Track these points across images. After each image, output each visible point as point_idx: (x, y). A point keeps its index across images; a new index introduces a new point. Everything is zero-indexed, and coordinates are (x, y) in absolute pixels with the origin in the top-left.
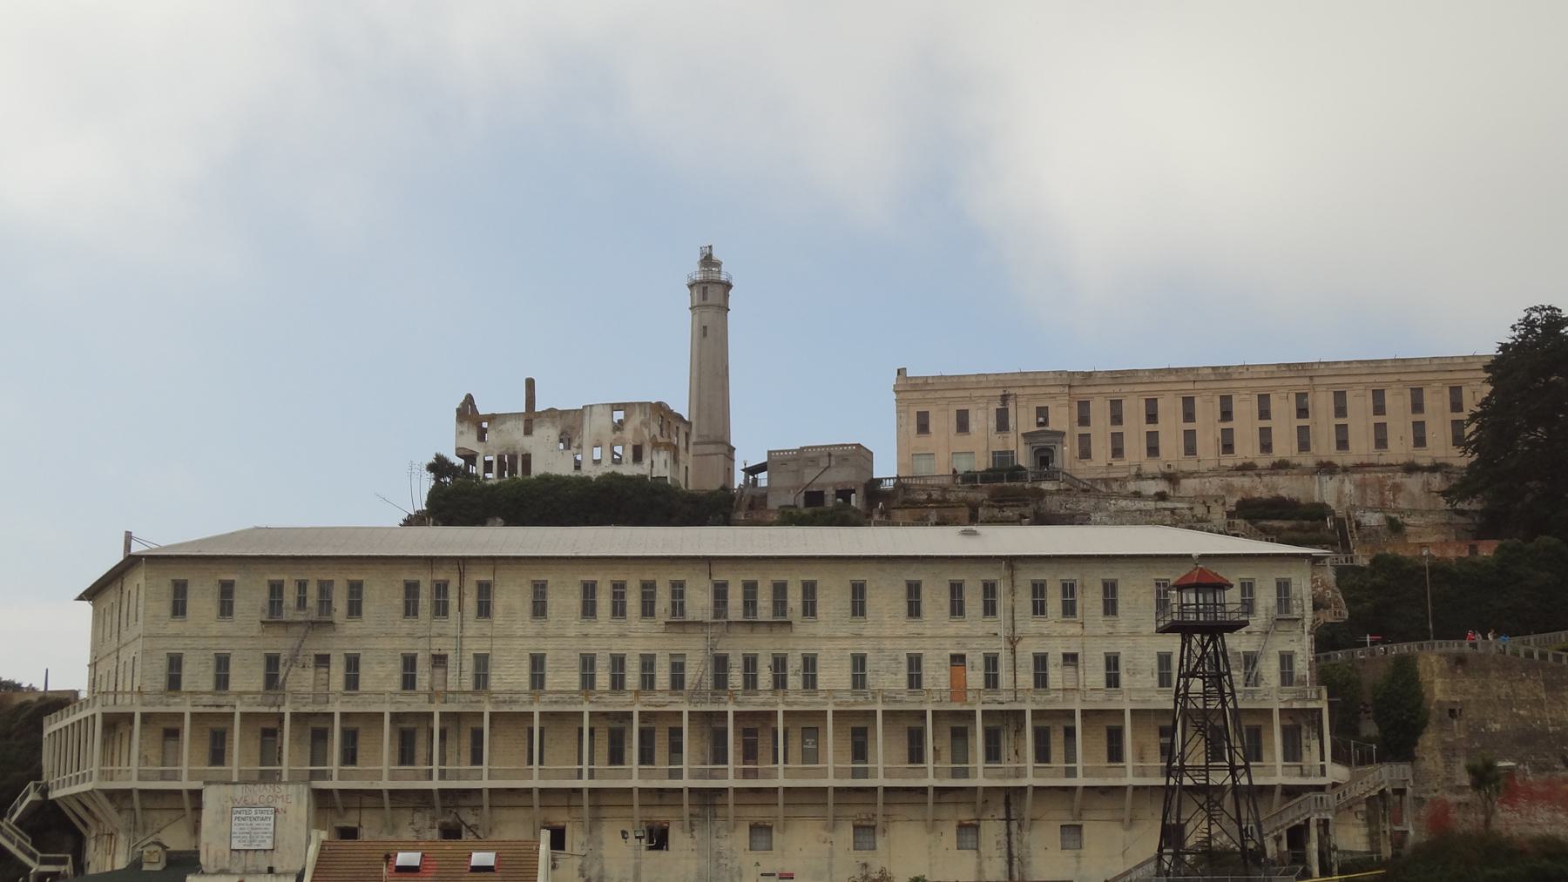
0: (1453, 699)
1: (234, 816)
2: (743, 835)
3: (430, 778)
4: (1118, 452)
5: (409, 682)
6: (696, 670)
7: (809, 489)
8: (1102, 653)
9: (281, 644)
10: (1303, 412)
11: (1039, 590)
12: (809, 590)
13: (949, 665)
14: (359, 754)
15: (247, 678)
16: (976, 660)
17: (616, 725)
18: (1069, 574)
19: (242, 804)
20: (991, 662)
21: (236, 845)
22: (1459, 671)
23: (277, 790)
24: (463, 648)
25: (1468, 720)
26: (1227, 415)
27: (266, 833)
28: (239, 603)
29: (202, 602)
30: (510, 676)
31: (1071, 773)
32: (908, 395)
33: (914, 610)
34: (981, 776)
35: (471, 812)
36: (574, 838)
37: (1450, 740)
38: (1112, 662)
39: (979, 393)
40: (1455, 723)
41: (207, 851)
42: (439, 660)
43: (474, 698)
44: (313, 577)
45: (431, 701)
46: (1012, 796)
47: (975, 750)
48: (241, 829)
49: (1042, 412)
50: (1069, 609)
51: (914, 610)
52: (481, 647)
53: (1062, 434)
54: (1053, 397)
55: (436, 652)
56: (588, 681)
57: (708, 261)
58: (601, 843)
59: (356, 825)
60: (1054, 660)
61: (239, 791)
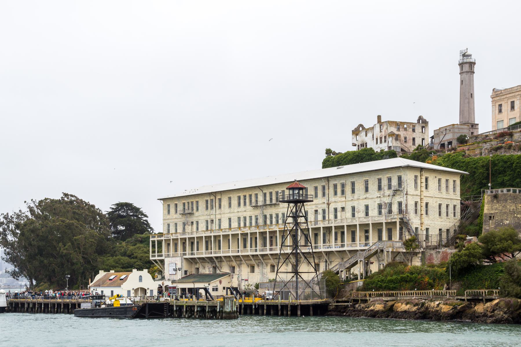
0: (491, 212)
2: (269, 268)
3: (212, 254)
6: (261, 221)
7: (441, 143)
8: (333, 208)
9: (183, 219)
11: (335, 186)
13: (314, 214)
14: (199, 248)
15: (180, 230)
16: (320, 211)
17: (245, 237)
18: (343, 181)
22: (495, 201)
25: (496, 220)
29: (172, 210)
30: (225, 225)
31: (343, 246)
32: (495, 99)
34: (322, 248)
36: (237, 270)
37: (487, 228)
38: (353, 208)
39: (517, 93)
40: (491, 221)
43: (218, 231)
44: (190, 200)
45: (211, 233)
46: (328, 253)
47: (248, 243)
50: (343, 192)
55: (211, 219)
56: (239, 224)
58: (242, 271)
60: (339, 209)
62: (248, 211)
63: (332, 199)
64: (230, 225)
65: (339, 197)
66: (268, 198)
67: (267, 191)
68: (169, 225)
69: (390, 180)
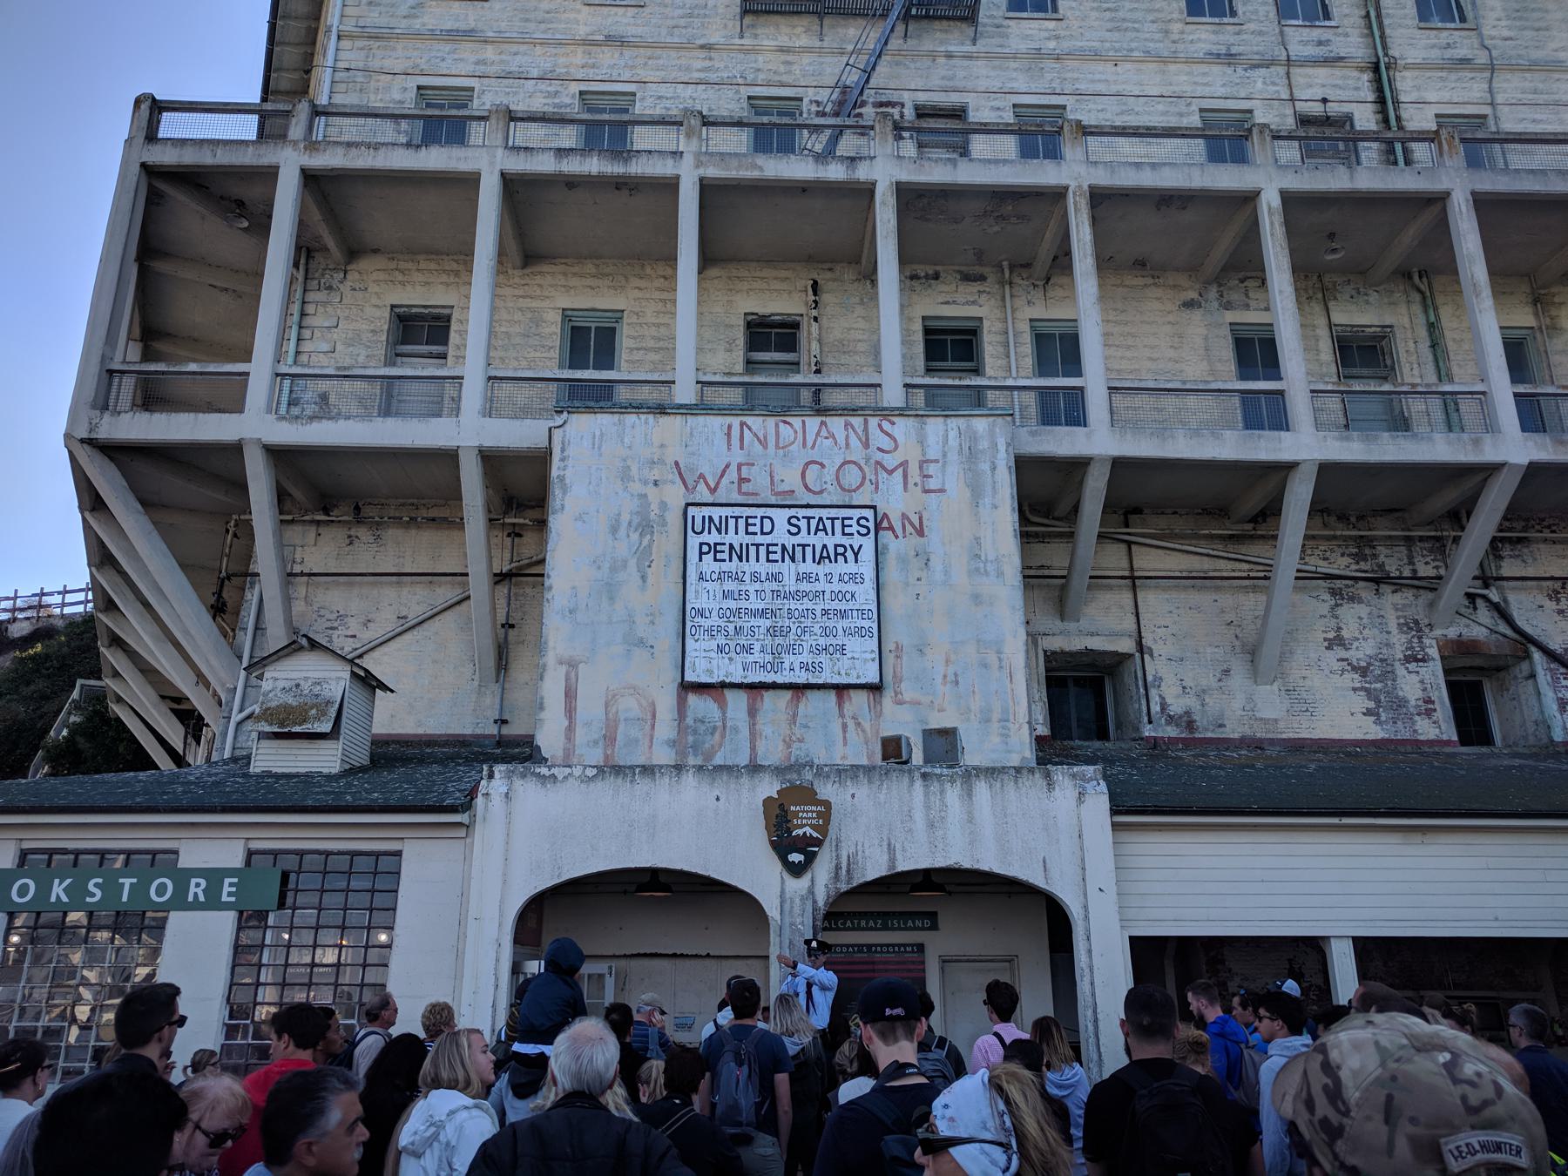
1: (694, 541)
19: (727, 492)
21: (705, 665)
23: (878, 439)
24: (1402, 98)
27: (843, 614)
35: (1550, 605)
41: (570, 695)
48: (726, 595)
55: (1316, 109)
59: (1126, 646)
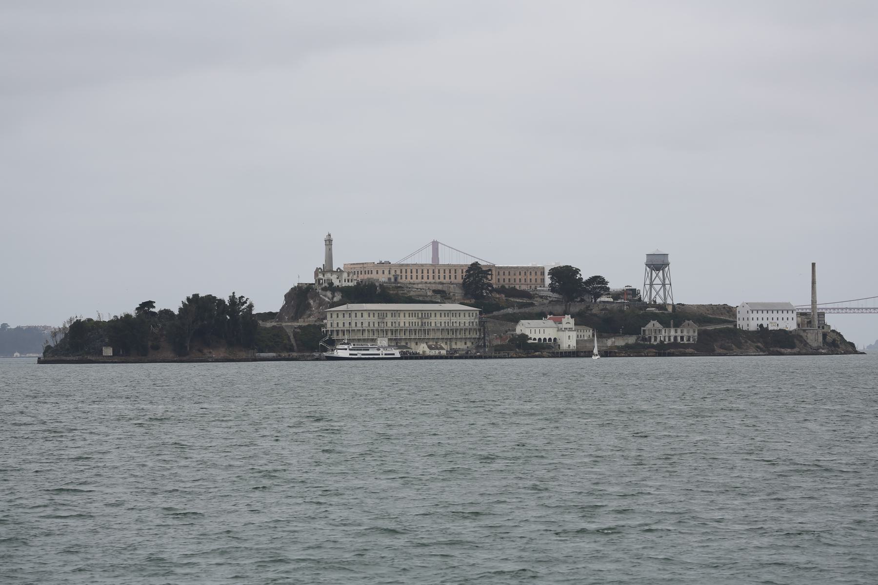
4: (406, 278)
5: (392, 325)
6: (420, 324)
10: (433, 273)
11: (453, 313)
12: (431, 313)
15: (376, 325)
16: (447, 322)
20: (448, 322)
26: (422, 273)
28: (375, 316)
29: (371, 315)
30: (402, 324)
33: (441, 316)
42: (395, 322)
44: (382, 312)
49: (396, 271)
50: (456, 316)
51: (441, 316)
52: (399, 321)
53: (398, 275)
54: (398, 269)
57: (329, 235)
61: (381, 338)
62: (415, 320)
63: (452, 318)
64: (405, 325)
65: (454, 318)
66: (424, 315)
67: (423, 312)
68: (369, 323)
69: (473, 313)
